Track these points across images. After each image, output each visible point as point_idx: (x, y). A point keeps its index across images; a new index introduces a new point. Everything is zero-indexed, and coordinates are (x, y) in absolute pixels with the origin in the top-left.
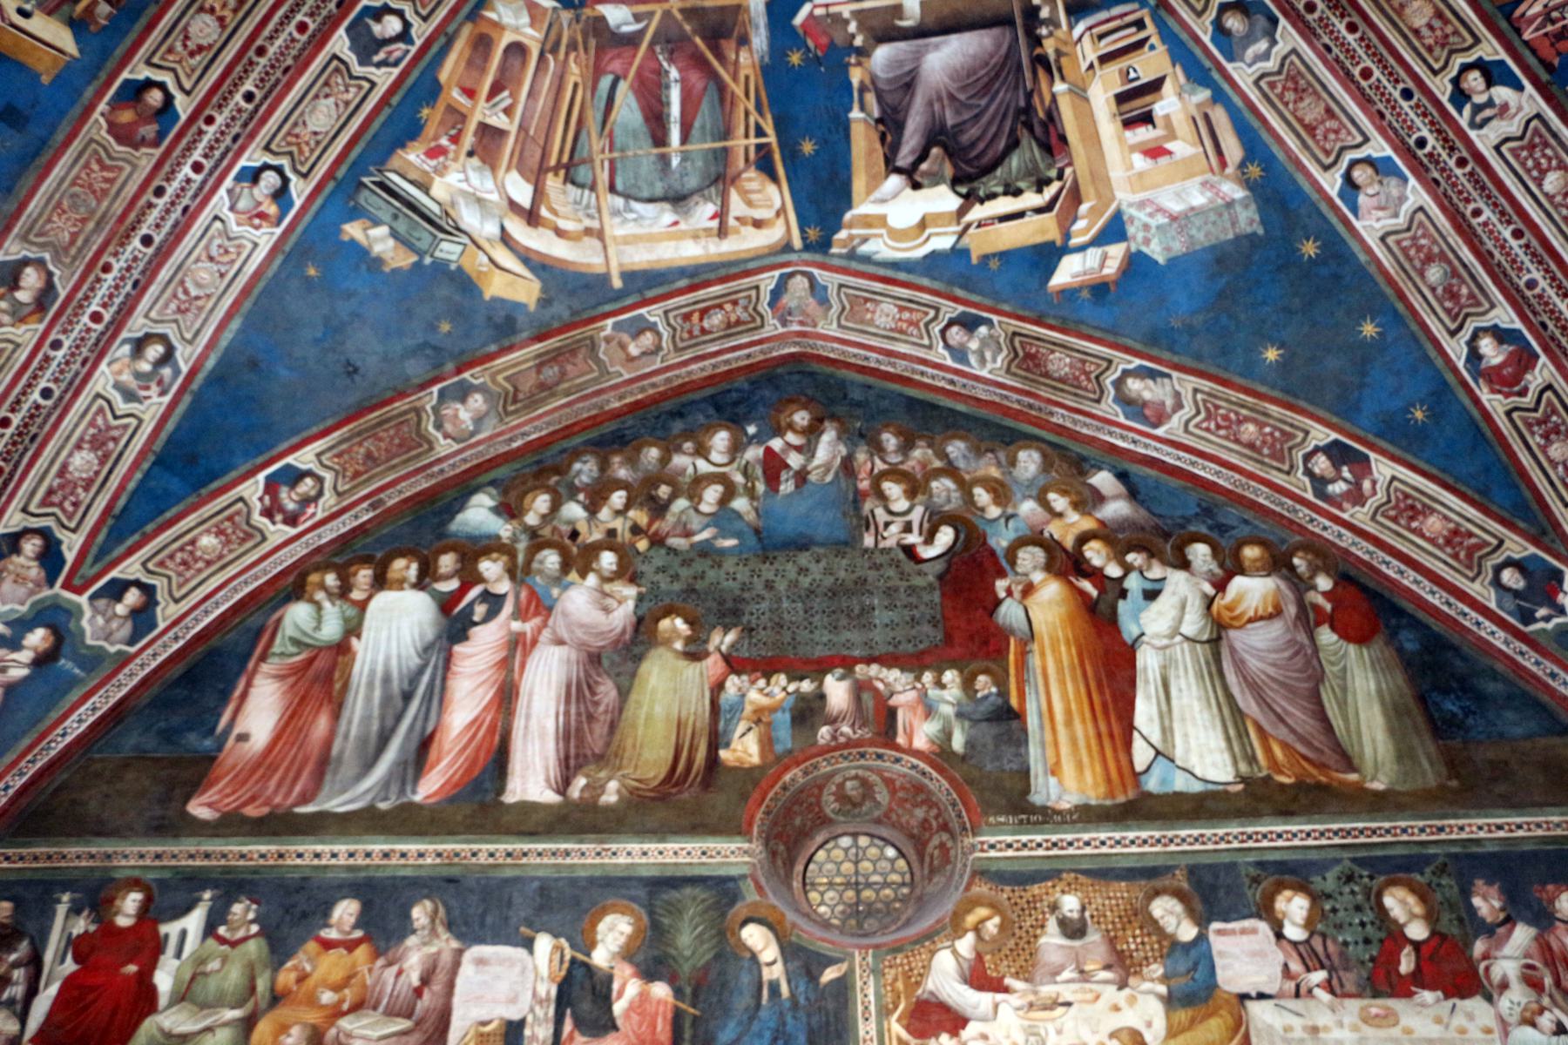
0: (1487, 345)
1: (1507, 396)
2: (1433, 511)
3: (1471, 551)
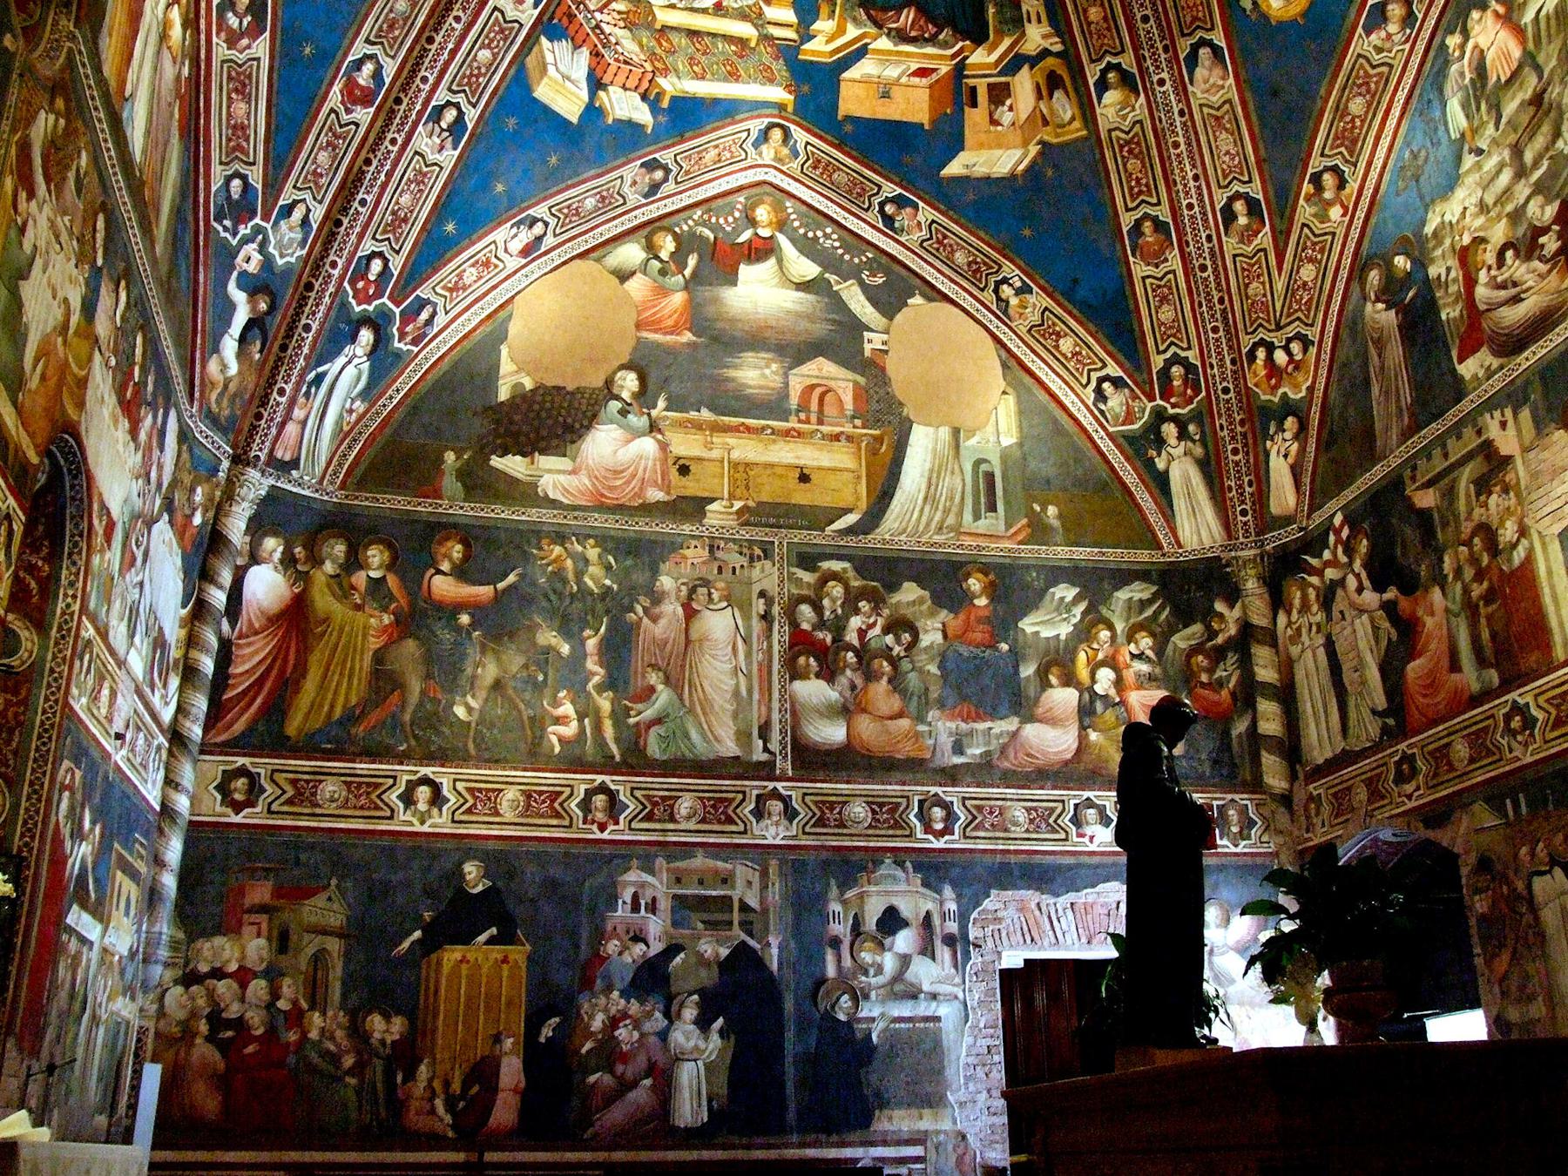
0: (368, 68)
1: (343, 102)
2: (249, 103)
3: (239, 148)
